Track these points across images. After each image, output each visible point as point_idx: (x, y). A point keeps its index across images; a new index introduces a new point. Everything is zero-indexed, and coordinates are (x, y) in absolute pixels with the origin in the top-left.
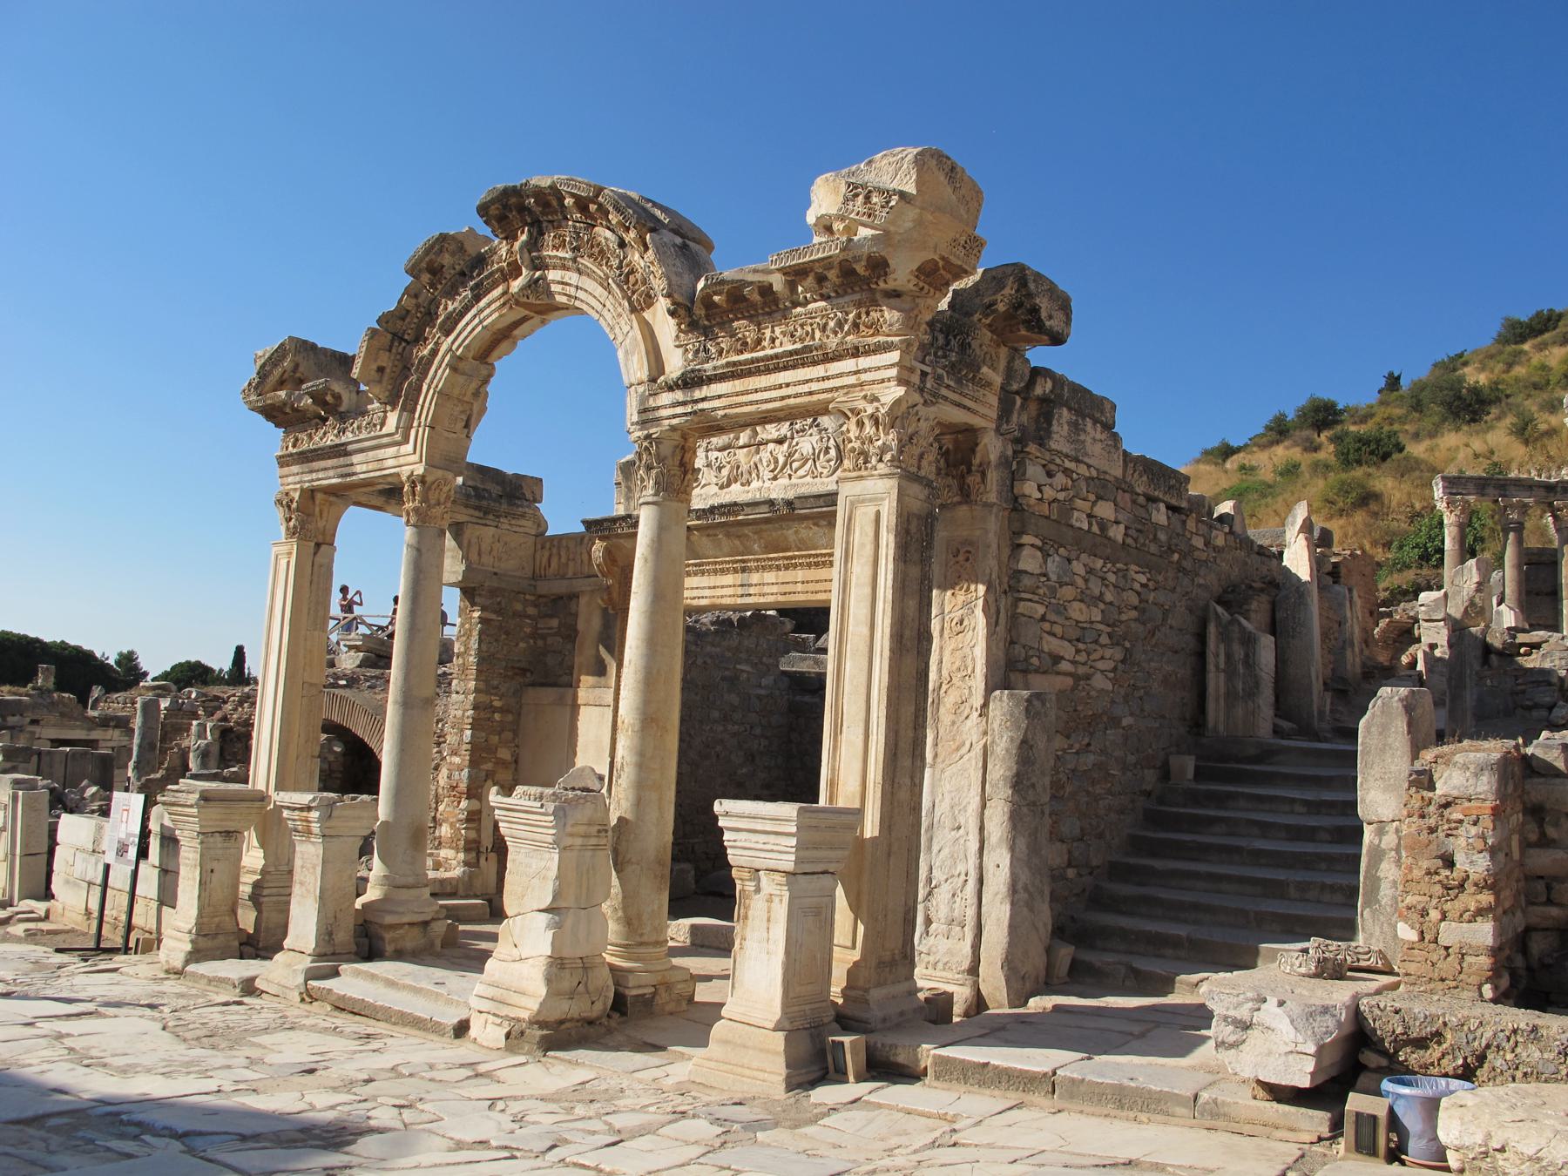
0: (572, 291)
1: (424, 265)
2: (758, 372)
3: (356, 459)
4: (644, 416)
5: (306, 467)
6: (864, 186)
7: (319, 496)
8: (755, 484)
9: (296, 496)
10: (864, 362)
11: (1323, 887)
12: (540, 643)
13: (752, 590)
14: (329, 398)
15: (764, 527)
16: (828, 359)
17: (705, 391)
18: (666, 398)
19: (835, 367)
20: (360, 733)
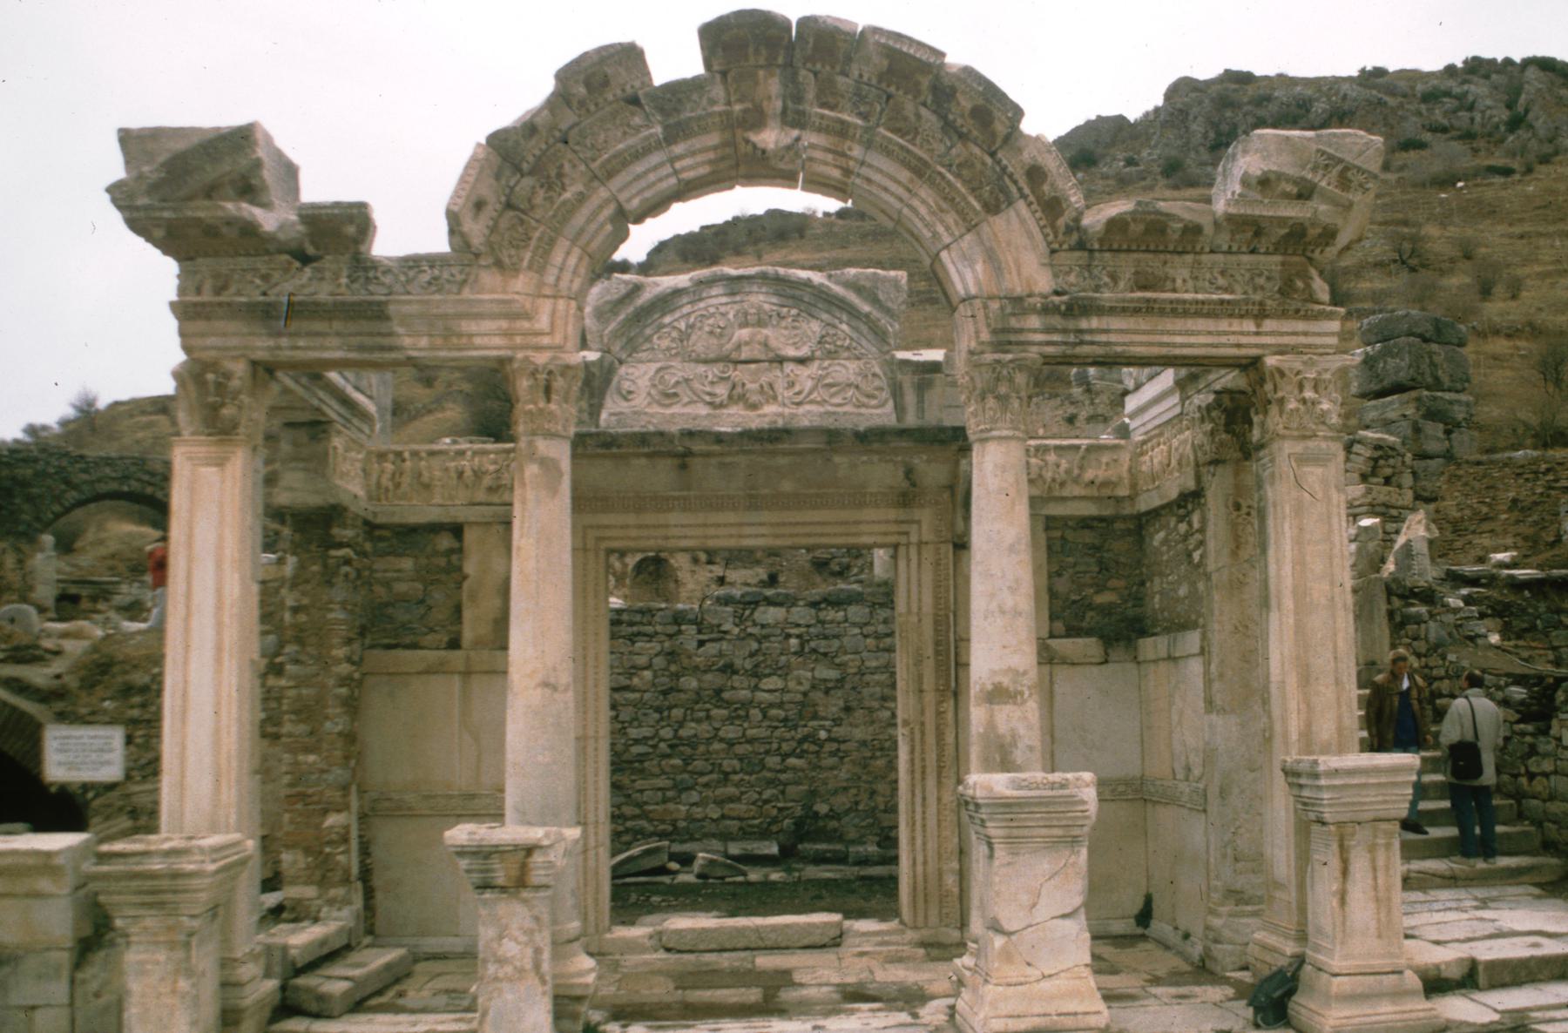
1: (582, 77)
4: (1003, 337)
6: (1341, 161)
9: (239, 369)
14: (351, 230)
17: (1095, 323)
18: (1034, 321)
19: (1269, 325)
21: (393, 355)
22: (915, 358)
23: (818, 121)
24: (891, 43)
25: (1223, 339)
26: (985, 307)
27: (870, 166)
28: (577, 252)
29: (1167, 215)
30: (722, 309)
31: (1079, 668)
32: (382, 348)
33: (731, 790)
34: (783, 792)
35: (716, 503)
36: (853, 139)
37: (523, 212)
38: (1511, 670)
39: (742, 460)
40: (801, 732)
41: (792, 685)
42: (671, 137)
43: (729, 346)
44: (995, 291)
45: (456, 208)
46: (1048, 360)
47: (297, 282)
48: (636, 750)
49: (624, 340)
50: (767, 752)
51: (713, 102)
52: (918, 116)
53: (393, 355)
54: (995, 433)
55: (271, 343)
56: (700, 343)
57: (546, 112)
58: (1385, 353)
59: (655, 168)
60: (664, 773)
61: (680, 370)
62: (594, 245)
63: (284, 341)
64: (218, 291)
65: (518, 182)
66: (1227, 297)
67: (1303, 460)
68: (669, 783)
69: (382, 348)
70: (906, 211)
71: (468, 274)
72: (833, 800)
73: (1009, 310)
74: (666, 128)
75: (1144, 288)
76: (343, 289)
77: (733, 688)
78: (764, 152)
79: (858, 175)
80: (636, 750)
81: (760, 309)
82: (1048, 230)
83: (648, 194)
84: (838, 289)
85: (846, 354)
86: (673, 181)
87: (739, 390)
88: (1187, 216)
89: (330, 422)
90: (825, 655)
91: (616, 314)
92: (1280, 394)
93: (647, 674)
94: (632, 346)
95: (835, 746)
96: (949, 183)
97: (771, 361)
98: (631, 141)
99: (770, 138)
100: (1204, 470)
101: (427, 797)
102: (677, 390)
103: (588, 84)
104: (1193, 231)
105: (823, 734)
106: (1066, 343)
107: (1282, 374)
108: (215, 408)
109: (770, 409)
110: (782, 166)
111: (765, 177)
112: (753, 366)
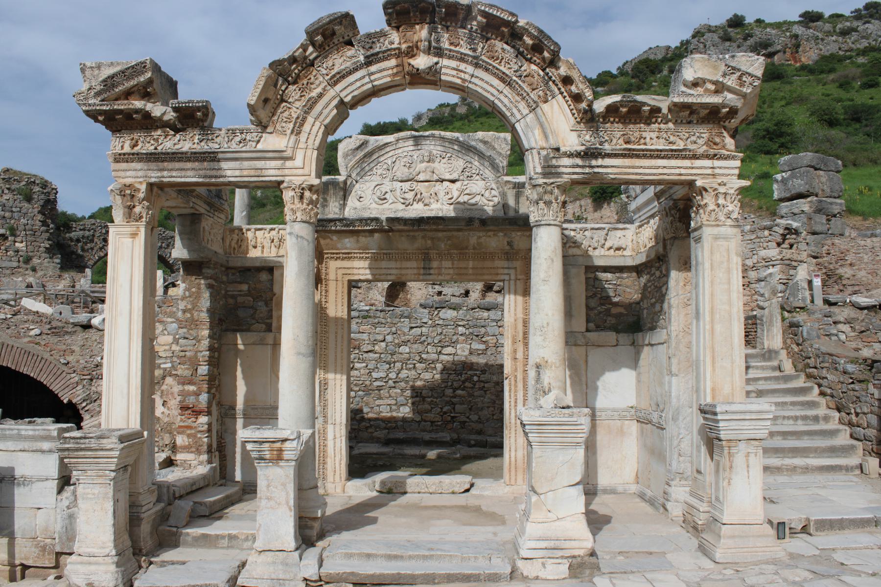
0: (467, 77)
2: (645, 157)
3: (224, 165)
4: (547, 170)
5: (153, 165)
6: (739, 70)
7: (155, 189)
8: (434, 206)
9: (143, 187)
10: (717, 163)
11: (784, 417)
12: (231, 301)
13: (432, 271)
15: (455, 233)
16: (695, 157)
17: (600, 162)
18: (566, 161)
20: (25, 370)
21: (221, 180)
22: (514, 180)
23: (448, 53)
24: (487, 9)
25: (673, 171)
26: (539, 154)
27: (477, 77)
28: (318, 124)
29: (641, 102)
30: (410, 153)
31: (602, 349)
32: (216, 177)
33: (427, 406)
34: (454, 408)
35: (404, 256)
36: (466, 62)
37: (289, 103)
38: (847, 354)
39: (421, 234)
40: (463, 378)
41: (459, 352)
42: (369, 62)
43: (414, 173)
44: (544, 145)
45: (252, 103)
46: (574, 183)
47: (172, 142)
48: (376, 384)
49: (359, 170)
50: (446, 387)
51: (392, 43)
52: (502, 49)
53: (221, 180)
54: (543, 223)
55: (159, 174)
56: (401, 171)
57: (301, 50)
58: (792, 177)
59: (360, 79)
60: (390, 396)
61: (387, 186)
62: (327, 121)
63: (165, 173)
64: (133, 146)
65: (286, 88)
66: (674, 147)
67: (716, 238)
68: (394, 402)
69: (216, 177)
70: (496, 102)
71: (261, 137)
72: (480, 413)
73: (552, 155)
74: (366, 57)
75: (627, 142)
76: (195, 146)
77: (428, 353)
78: (418, 70)
79: (470, 82)
80: (376, 384)
81: (430, 152)
82: (574, 111)
83: (356, 93)
84: (473, 143)
85: (478, 177)
86: (370, 86)
87: (419, 196)
88: (652, 103)
89: (201, 214)
90: (477, 336)
91: (355, 156)
92: (705, 201)
93: (383, 344)
94: (362, 174)
95: (482, 384)
96: (520, 86)
97: (436, 181)
98: (348, 64)
99: (422, 62)
100: (668, 242)
101: (253, 409)
102: (387, 196)
103: (323, 35)
104: (656, 110)
105: (475, 378)
106: (584, 173)
107: (706, 190)
108: (131, 208)
109: (434, 206)
110: (428, 77)
111: (421, 84)
112: (426, 184)
